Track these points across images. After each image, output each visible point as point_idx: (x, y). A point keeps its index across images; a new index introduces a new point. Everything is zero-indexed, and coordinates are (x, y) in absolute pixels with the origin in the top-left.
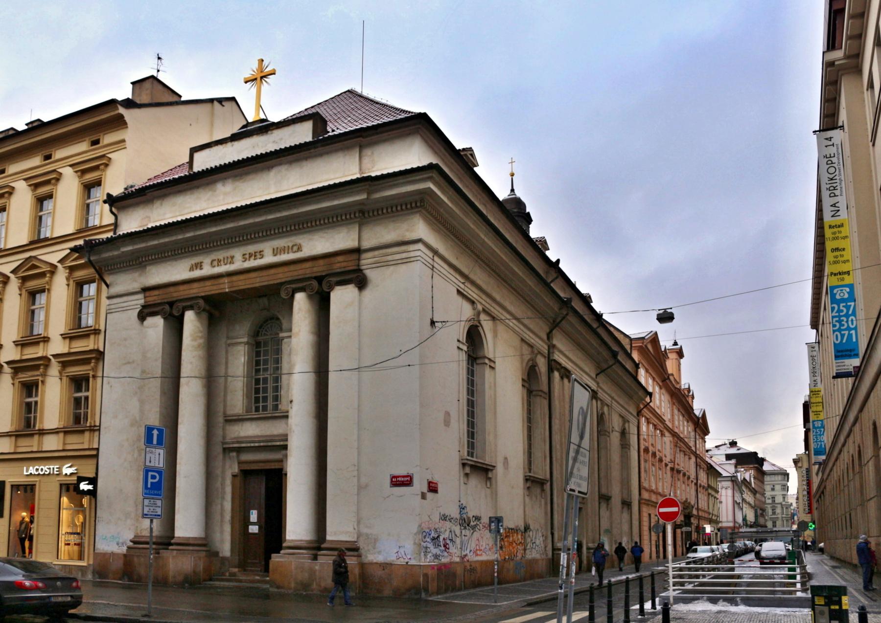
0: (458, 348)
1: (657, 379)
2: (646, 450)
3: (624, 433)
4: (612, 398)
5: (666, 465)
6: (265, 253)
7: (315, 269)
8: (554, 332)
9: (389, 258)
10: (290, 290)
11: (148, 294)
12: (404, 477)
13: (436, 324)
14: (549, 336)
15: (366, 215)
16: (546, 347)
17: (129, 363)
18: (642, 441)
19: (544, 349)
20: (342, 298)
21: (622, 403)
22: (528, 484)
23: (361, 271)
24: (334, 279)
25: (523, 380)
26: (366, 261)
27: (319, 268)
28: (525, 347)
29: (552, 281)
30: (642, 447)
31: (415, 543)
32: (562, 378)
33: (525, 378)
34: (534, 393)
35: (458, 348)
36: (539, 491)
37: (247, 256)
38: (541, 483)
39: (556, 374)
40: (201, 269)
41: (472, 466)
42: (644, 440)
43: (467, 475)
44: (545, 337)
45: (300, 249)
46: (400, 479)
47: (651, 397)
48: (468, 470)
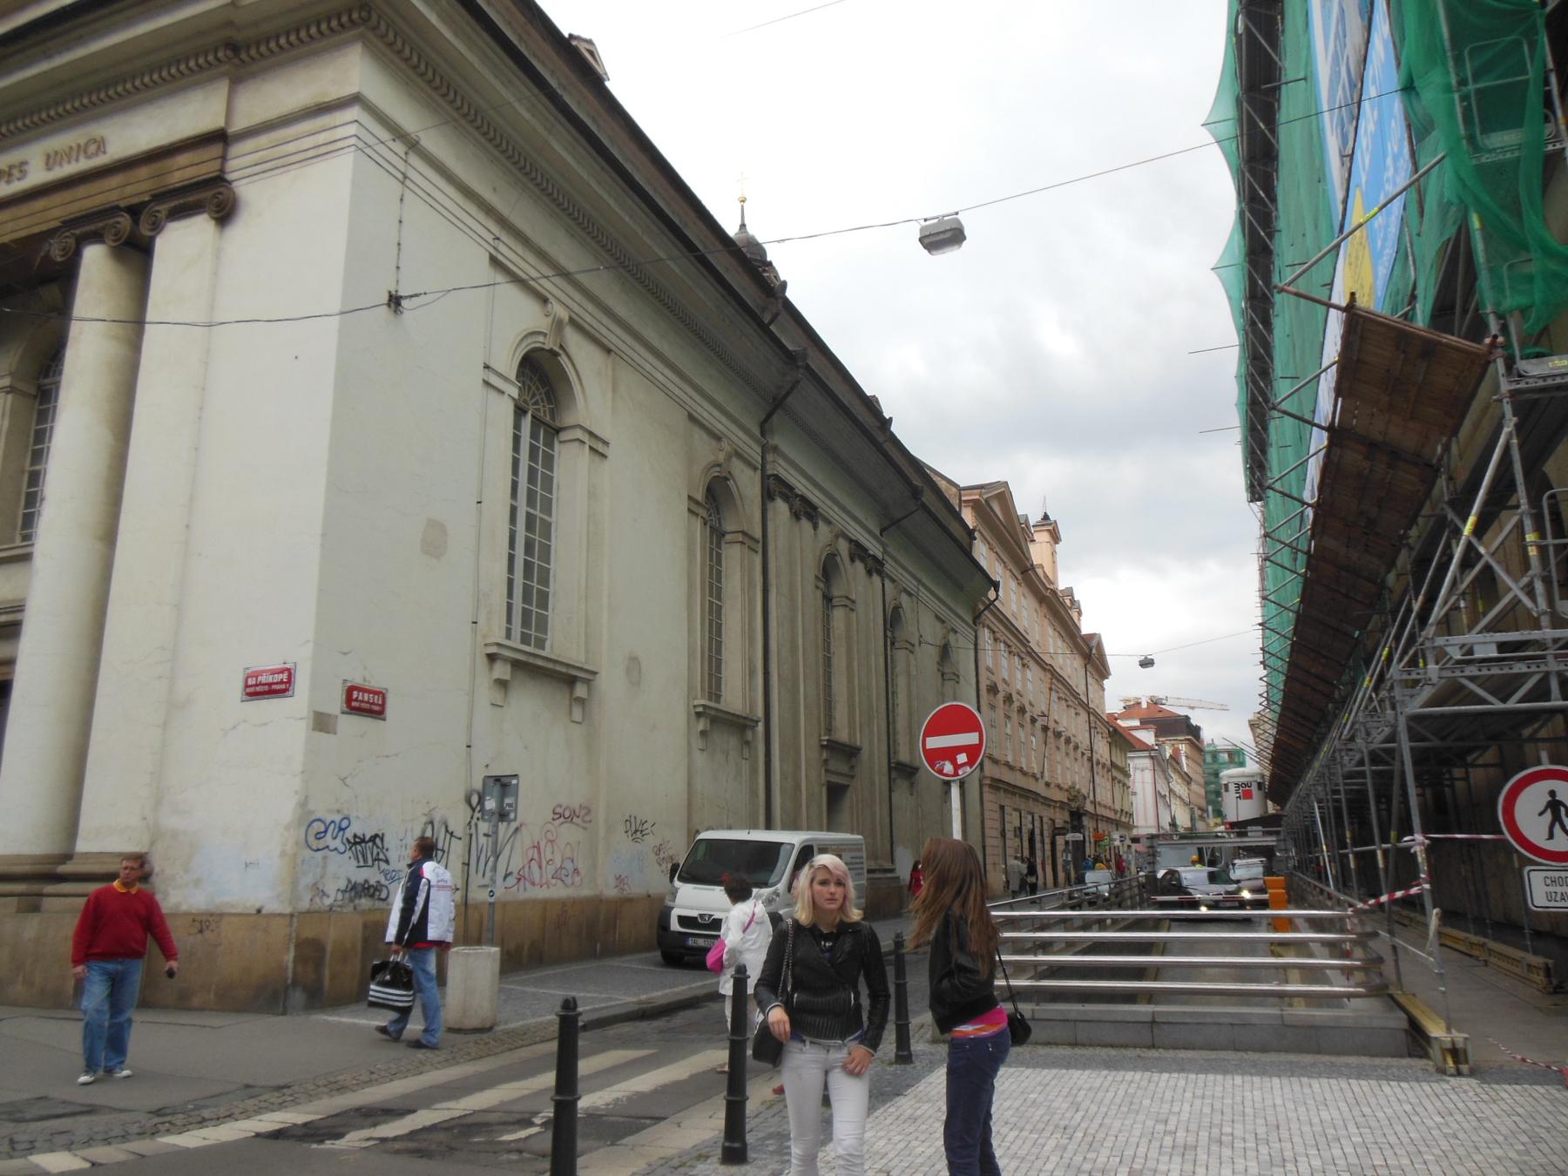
0: (487, 383)
1: (1010, 566)
2: (993, 689)
3: (945, 652)
4: (919, 581)
5: (1033, 720)
6: (31, 168)
7: (129, 190)
8: (775, 418)
9: (290, 148)
10: (72, 241)
12: (274, 672)
13: (404, 303)
14: (764, 426)
15: (243, 56)
16: (759, 450)
18: (982, 671)
19: (755, 453)
21: (942, 595)
22: (702, 725)
23: (219, 180)
24: (164, 208)
25: (690, 498)
26: (240, 159)
28: (699, 436)
29: (771, 322)
30: (984, 684)
31: (283, 854)
32: (796, 516)
33: (700, 497)
34: (728, 537)
35: (487, 383)
36: (733, 742)
38: (738, 725)
39: (781, 508)
41: (517, 665)
42: (988, 669)
43: (502, 684)
44: (756, 431)
45: (101, 145)
46: (263, 679)
47: (997, 591)
48: (502, 671)
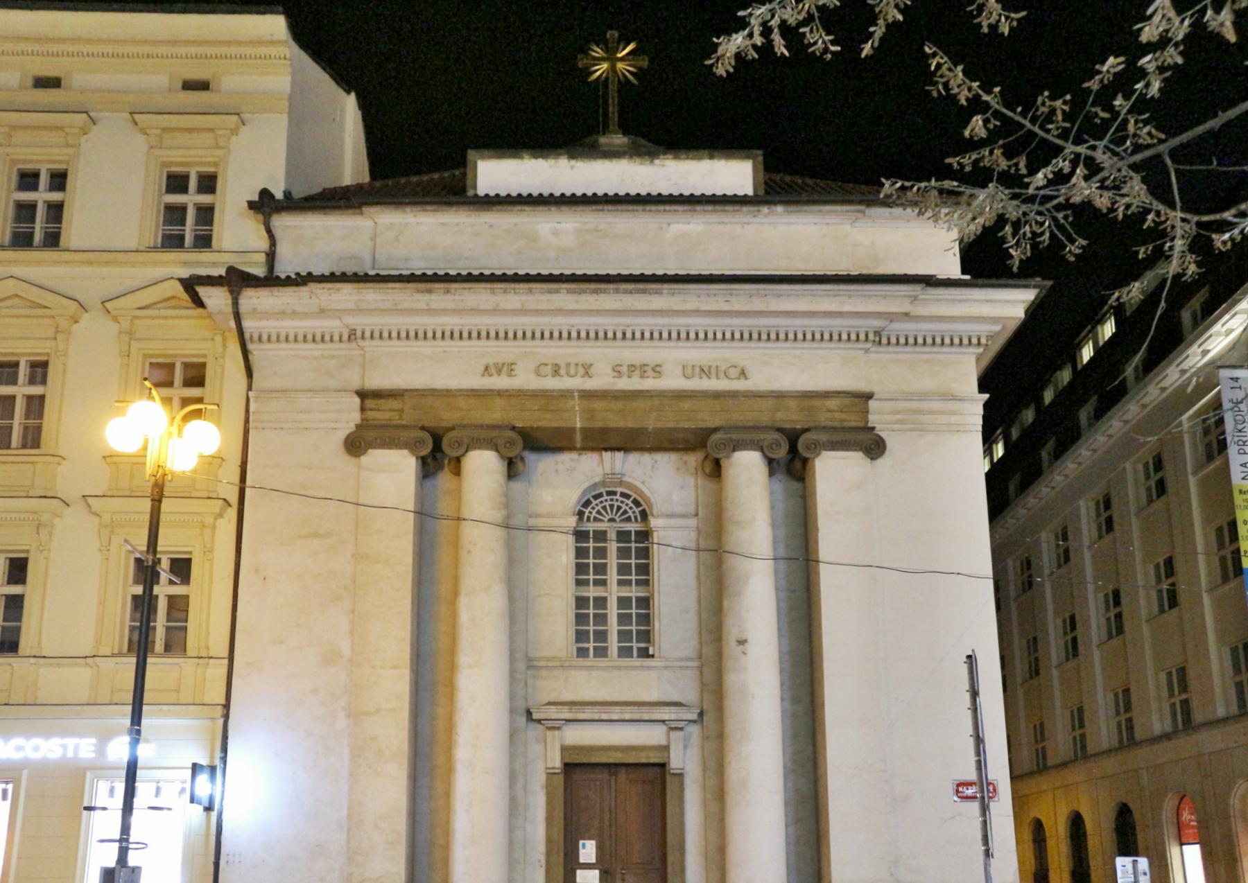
11: (370, 403)
17: (315, 535)
20: (834, 472)
27: (791, 417)
37: (624, 369)
40: (510, 375)
